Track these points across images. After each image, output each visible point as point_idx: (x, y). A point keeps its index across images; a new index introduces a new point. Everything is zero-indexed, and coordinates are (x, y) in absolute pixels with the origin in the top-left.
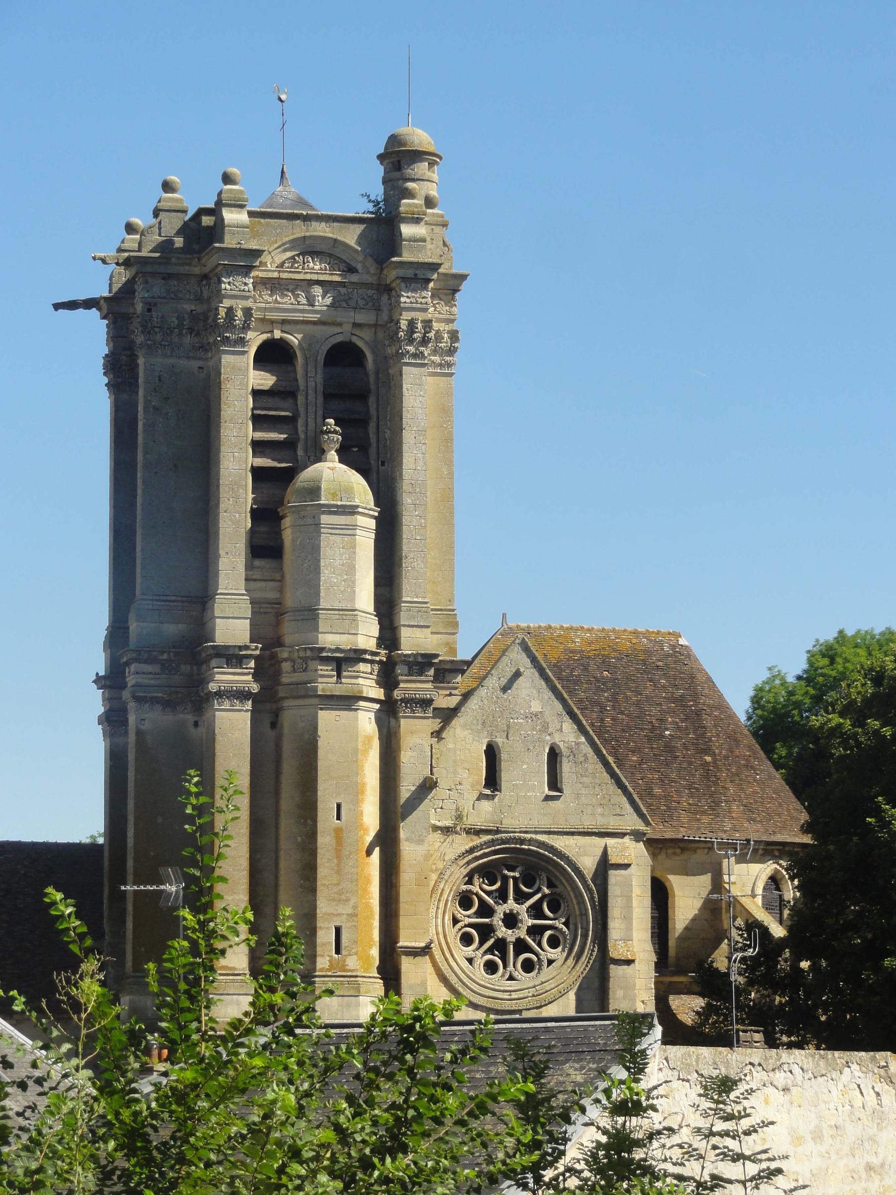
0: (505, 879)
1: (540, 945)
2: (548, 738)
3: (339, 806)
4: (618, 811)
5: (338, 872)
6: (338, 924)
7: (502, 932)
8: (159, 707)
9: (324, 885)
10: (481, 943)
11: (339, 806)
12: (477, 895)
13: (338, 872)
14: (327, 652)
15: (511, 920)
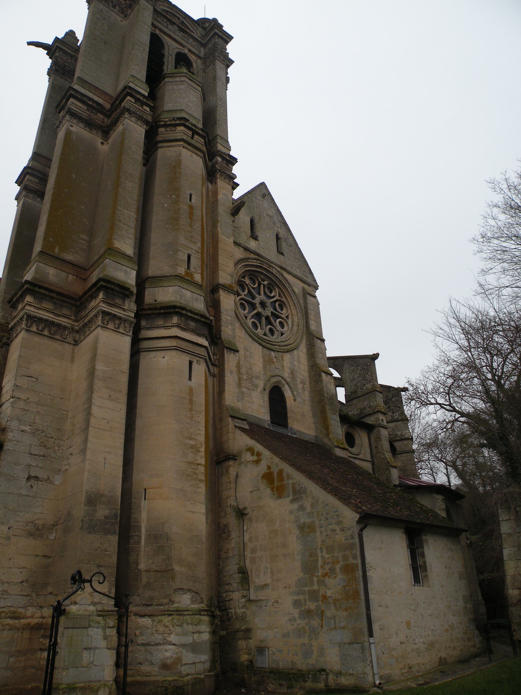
0: (259, 284)
1: (275, 322)
2: (276, 228)
3: (191, 195)
4: (305, 274)
5: (191, 226)
6: (189, 252)
7: (260, 309)
8: (82, 125)
9: (183, 229)
10: (249, 312)
11: (191, 195)
12: (247, 285)
13: (191, 226)
14: (189, 123)
15: (263, 304)
